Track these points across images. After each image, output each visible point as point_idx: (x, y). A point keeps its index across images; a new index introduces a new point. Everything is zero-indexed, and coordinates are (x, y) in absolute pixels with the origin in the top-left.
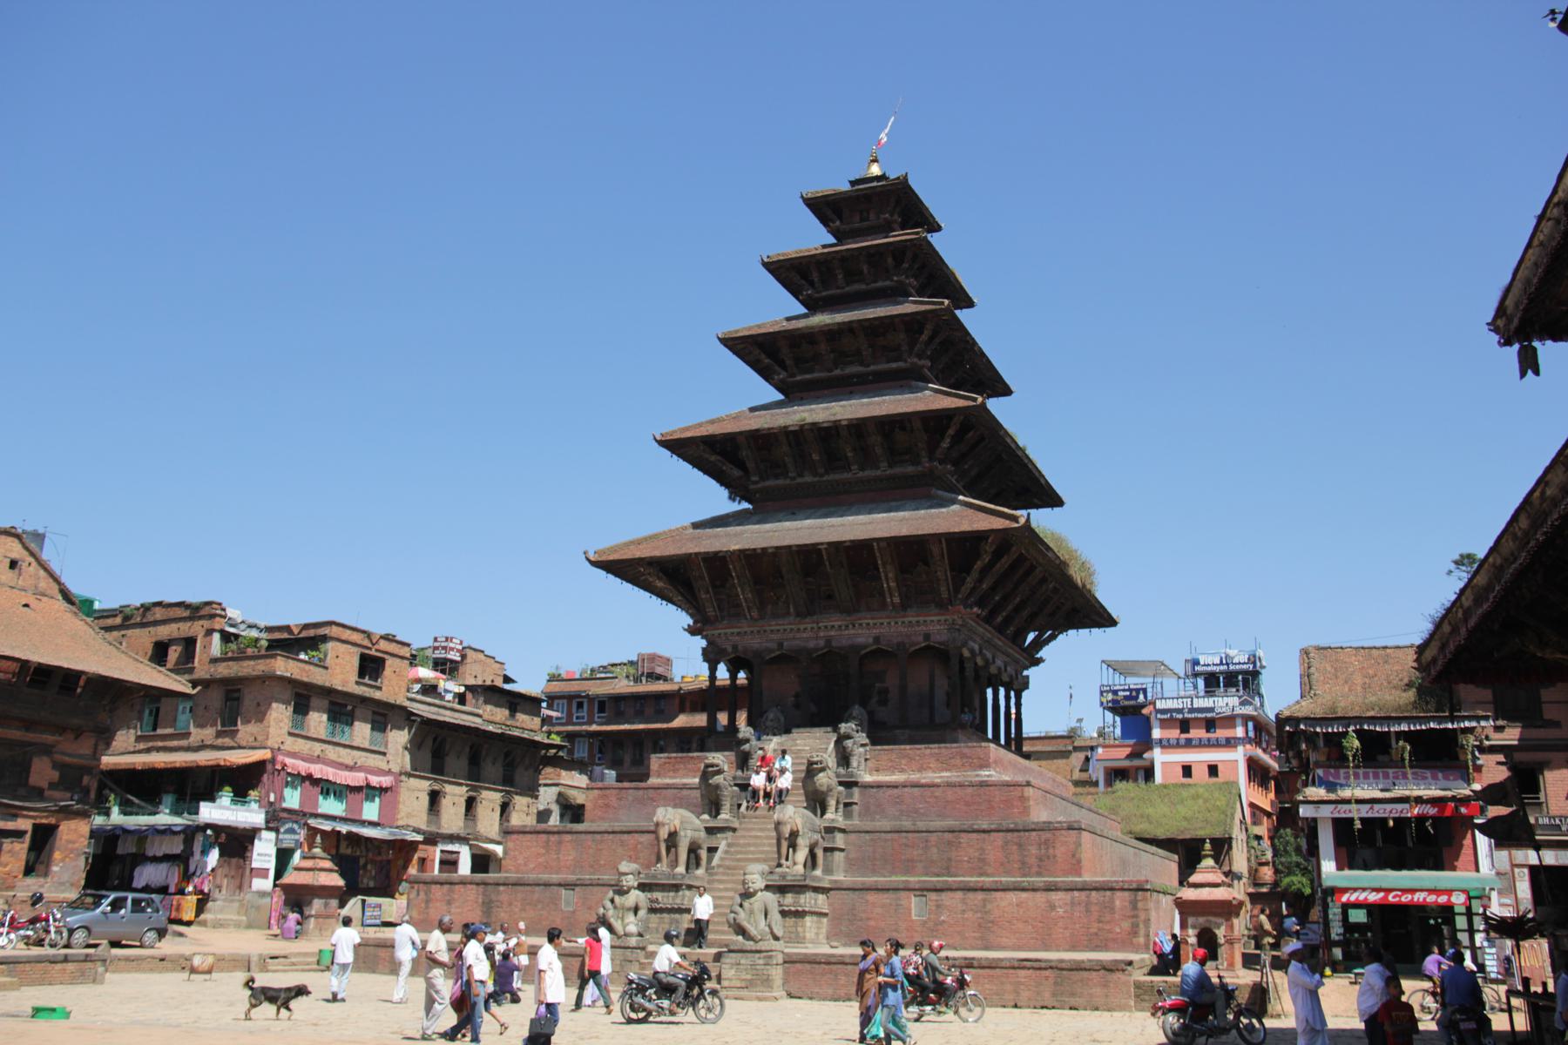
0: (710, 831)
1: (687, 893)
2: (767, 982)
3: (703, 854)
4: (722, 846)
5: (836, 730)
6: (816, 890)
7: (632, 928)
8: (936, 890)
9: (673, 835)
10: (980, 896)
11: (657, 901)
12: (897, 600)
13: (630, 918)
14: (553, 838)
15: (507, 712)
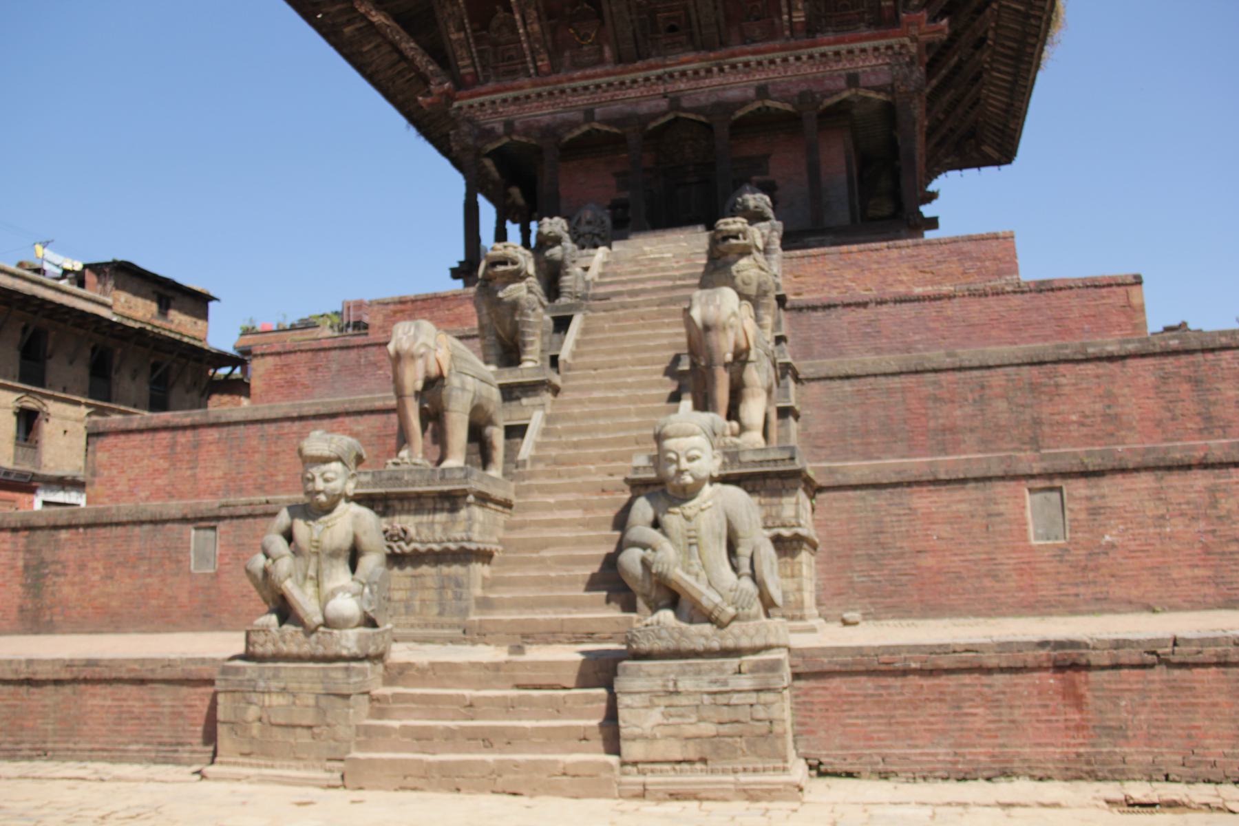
0: (510, 392)
1: (477, 512)
2: (764, 741)
3: (497, 436)
4: (536, 422)
5: (710, 226)
6: (814, 490)
7: (346, 605)
8: (1085, 474)
9: (434, 384)
10: (1200, 480)
11: (404, 535)
12: (799, 17)
13: (340, 576)
14: (184, 438)
15: (154, 307)
